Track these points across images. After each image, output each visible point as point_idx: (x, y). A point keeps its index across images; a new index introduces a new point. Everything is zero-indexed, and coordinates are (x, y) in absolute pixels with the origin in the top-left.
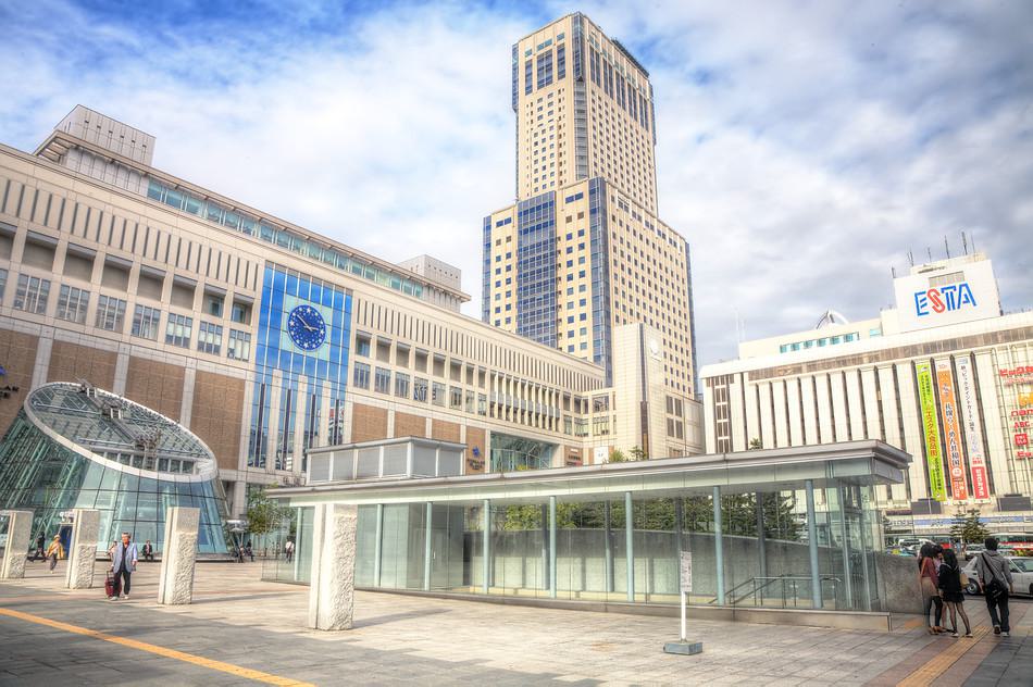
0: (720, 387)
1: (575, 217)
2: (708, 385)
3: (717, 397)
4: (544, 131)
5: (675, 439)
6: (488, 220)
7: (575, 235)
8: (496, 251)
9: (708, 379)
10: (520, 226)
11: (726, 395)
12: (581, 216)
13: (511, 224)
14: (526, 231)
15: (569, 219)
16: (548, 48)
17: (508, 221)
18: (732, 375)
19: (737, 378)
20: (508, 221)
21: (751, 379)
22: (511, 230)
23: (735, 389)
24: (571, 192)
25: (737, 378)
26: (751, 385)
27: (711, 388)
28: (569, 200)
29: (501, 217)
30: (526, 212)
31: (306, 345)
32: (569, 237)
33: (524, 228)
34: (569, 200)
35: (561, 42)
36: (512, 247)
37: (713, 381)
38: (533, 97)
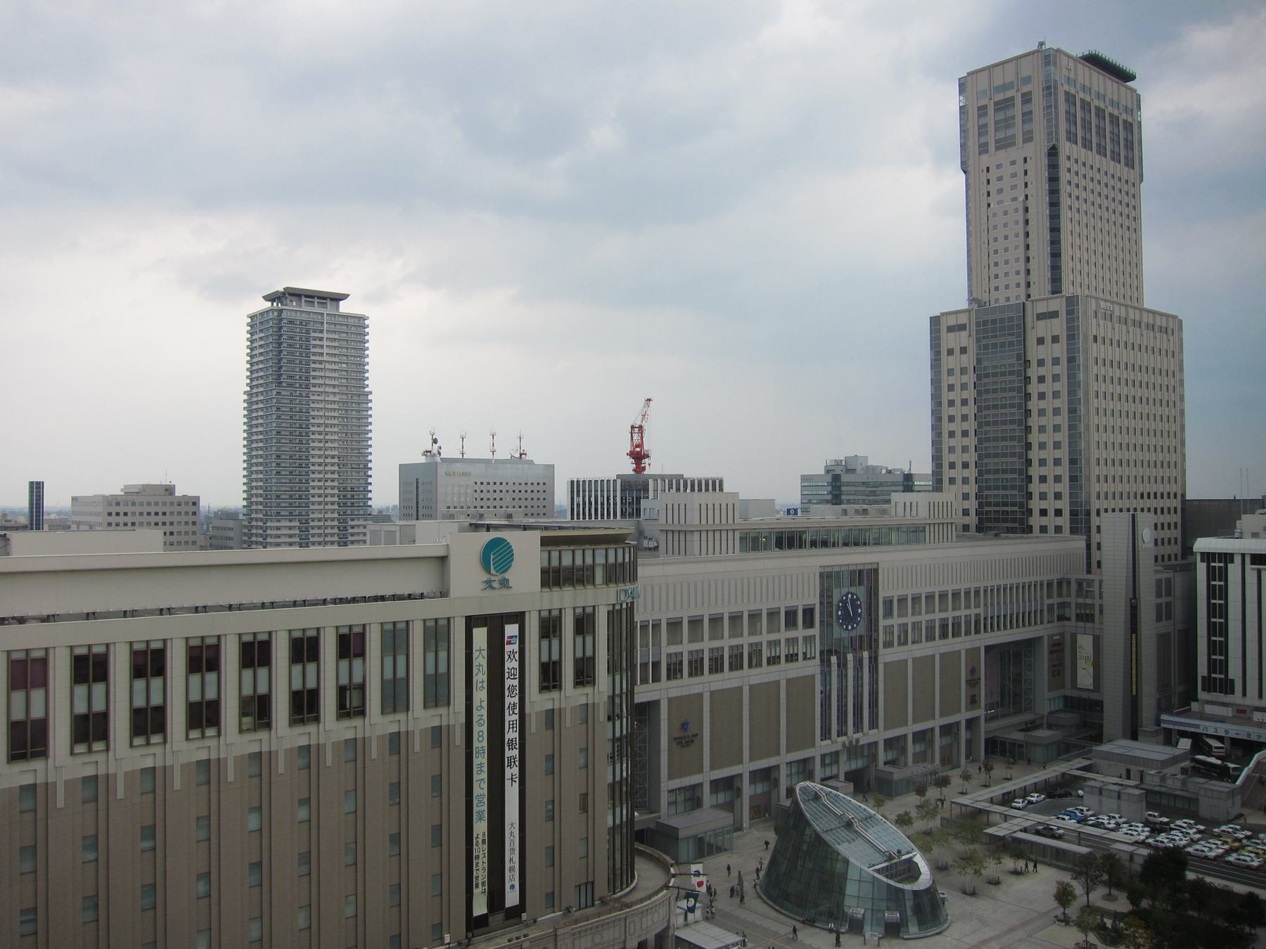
0: (1216, 564)
1: (1048, 340)
2: (1202, 561)
3: (1211, 573)
4: (1006, 213)
5: (1164, 623)
6: (935, 321)
7: (1049, 362)
8: (948, 362)
9: (1202, 554)
10: (978, 340)
11: (1223, 574)
12: (1055, 339)
13: (964, 334)
14: (986, 347)
15: (1041, 341)
16: (1009, 94)
17: (962, 327)
18: (1232, 555)
19: (1238, 559)
20: (962, 327)
21: (1253, 563)
22: (964, 339)
23: (1234, 570)
24: (1042, 308)
25: (1238, 559)
26: (1252, 569)
27: (1205, 564)
28: (1041, 317)
29: (952, 321)
30: (985, 323)
31: (850, 627)
32: (1041, 363)
33: (984, 342)
34: (1041, 317)
35: (1025, 89)
36: (968, 360)
37: (1208, 557)
38: (986, 160)
